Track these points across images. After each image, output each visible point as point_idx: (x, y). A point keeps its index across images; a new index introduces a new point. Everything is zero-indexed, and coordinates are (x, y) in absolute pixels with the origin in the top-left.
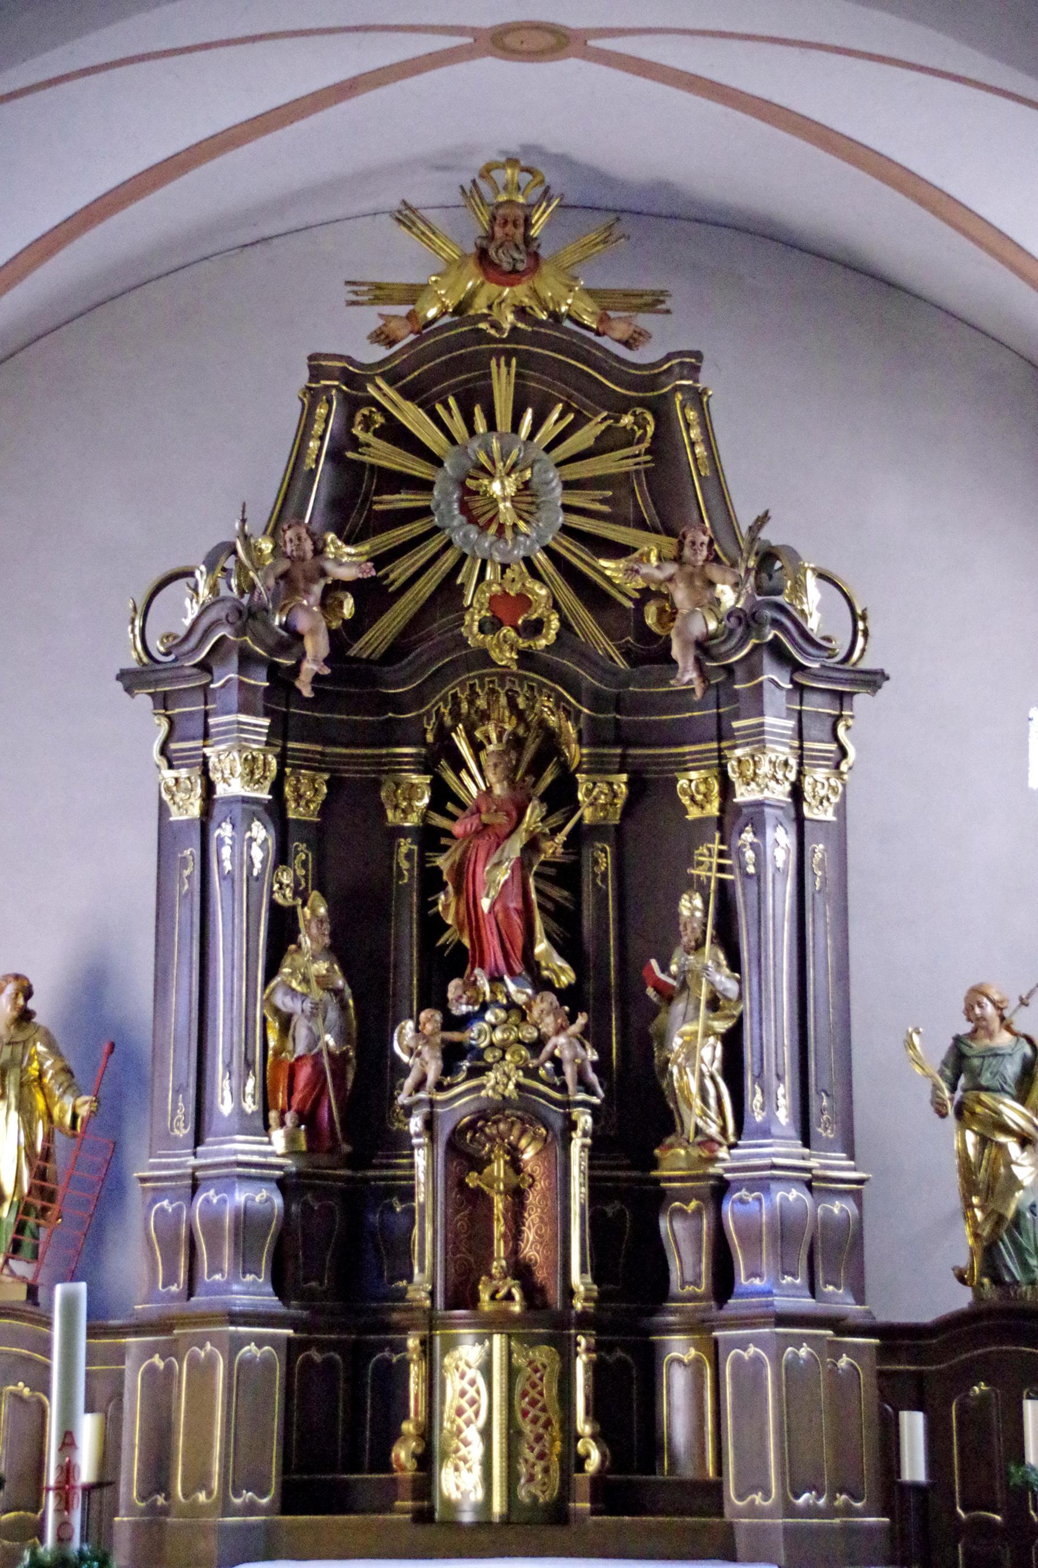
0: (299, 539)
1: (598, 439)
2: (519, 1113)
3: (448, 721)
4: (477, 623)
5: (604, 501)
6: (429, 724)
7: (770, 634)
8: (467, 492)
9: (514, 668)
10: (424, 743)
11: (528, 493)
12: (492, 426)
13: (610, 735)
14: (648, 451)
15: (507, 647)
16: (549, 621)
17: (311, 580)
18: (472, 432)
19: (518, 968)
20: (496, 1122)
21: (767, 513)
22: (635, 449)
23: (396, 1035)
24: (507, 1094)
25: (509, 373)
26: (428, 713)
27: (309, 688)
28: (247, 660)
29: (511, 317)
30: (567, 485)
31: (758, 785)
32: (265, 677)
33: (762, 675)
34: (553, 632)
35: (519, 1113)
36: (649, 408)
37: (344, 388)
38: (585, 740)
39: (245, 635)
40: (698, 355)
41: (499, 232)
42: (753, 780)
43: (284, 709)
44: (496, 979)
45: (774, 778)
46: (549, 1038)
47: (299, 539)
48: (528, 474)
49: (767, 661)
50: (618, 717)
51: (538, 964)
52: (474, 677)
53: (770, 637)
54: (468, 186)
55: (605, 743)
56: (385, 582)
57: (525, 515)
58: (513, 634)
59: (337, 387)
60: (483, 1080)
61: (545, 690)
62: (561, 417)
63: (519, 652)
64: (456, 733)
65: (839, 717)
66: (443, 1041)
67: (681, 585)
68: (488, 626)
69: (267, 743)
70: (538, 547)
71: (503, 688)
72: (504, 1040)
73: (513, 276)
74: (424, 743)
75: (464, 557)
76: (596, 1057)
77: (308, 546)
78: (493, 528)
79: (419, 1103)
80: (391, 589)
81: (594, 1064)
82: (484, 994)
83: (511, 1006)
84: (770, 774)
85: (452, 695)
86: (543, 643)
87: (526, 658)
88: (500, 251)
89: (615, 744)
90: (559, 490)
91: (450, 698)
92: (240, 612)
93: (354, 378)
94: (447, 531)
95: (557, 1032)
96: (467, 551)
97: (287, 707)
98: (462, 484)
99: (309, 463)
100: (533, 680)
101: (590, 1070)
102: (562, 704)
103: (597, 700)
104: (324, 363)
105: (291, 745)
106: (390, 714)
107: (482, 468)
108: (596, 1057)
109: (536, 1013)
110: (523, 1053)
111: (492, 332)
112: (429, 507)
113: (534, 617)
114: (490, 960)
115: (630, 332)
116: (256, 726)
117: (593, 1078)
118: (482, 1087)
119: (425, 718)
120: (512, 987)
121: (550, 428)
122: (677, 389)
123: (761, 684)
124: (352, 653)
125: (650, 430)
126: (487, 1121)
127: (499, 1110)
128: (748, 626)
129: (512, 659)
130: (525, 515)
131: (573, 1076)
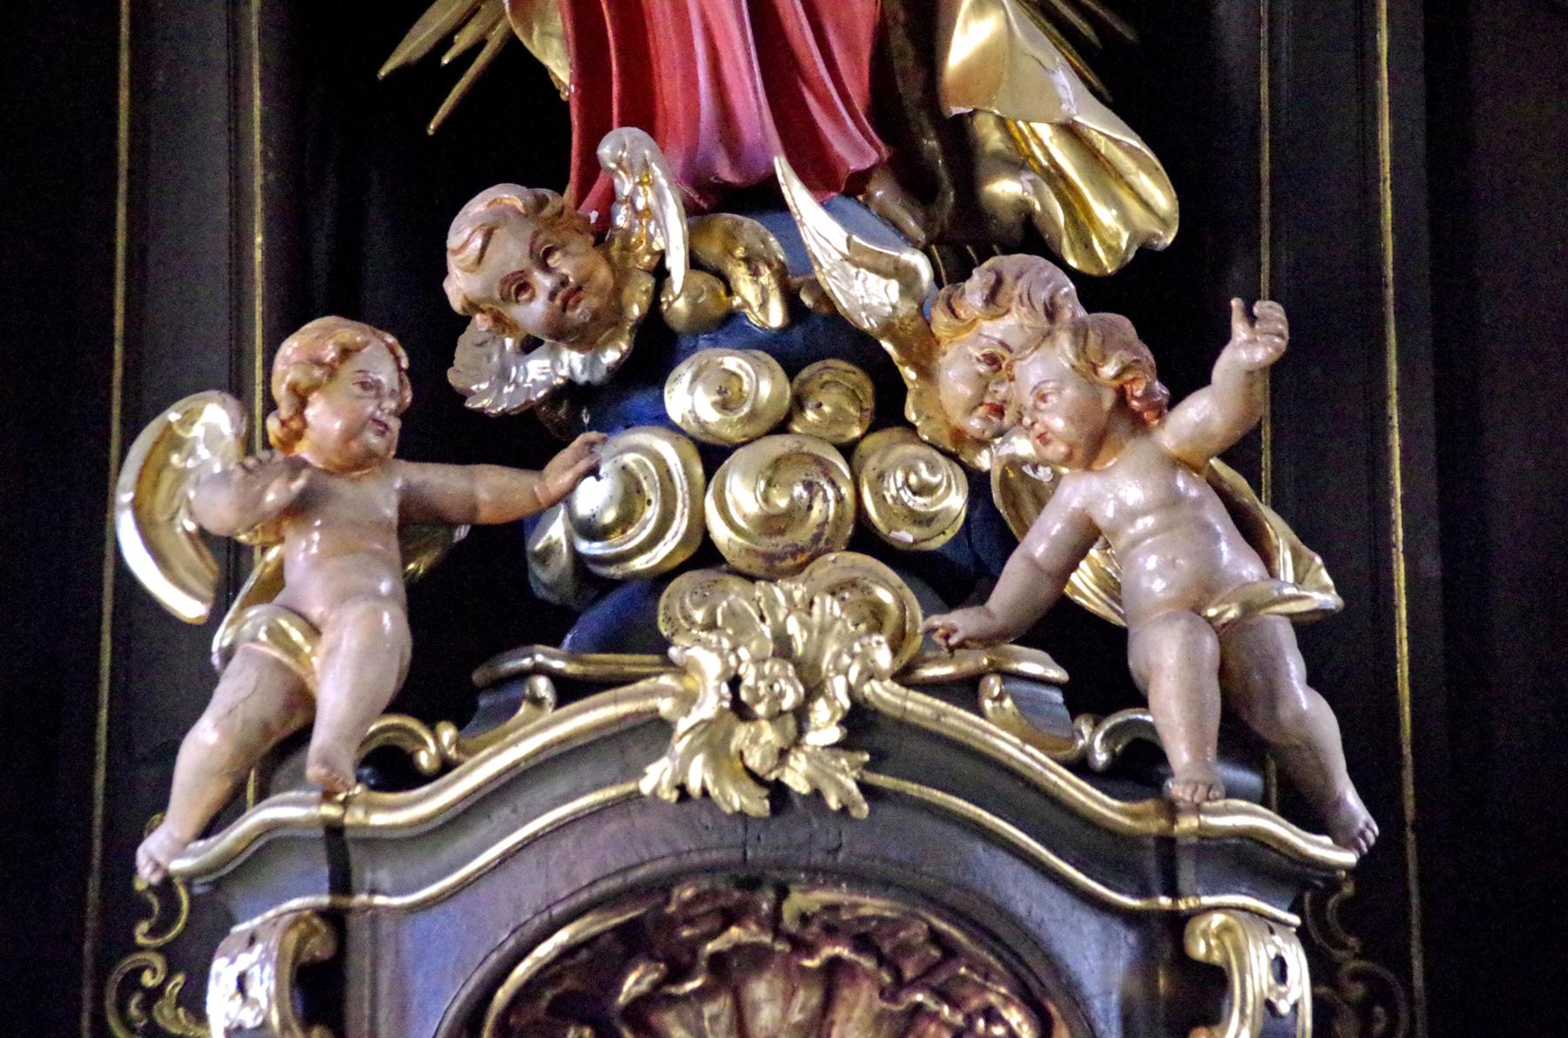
2: (873, 905)
19: (854, 148)
20: (727, 973)
23: (125, 497)
24: (796, 777)
35: (873, 905)
44: (729, 197)
46: (1040, 496)
51: (958, 134)
60: (656, 695)
66: (416, 521)
72: (772, 523)
76: (1323, 596)
79: (273, 842)
81: (1310, 630)
82: (660, 273)
83: (815, 334)
95: (1093, 448)
101: (1295, 667)
108: (1323, 596)
109: (956, 375)
110: (885, 596)
114: (681, 85)
117: (1311, 713)
118: (652, 732)
120: (818, 225)
126: (678, 973)
127: (745, 884)
131: (1193, 696)
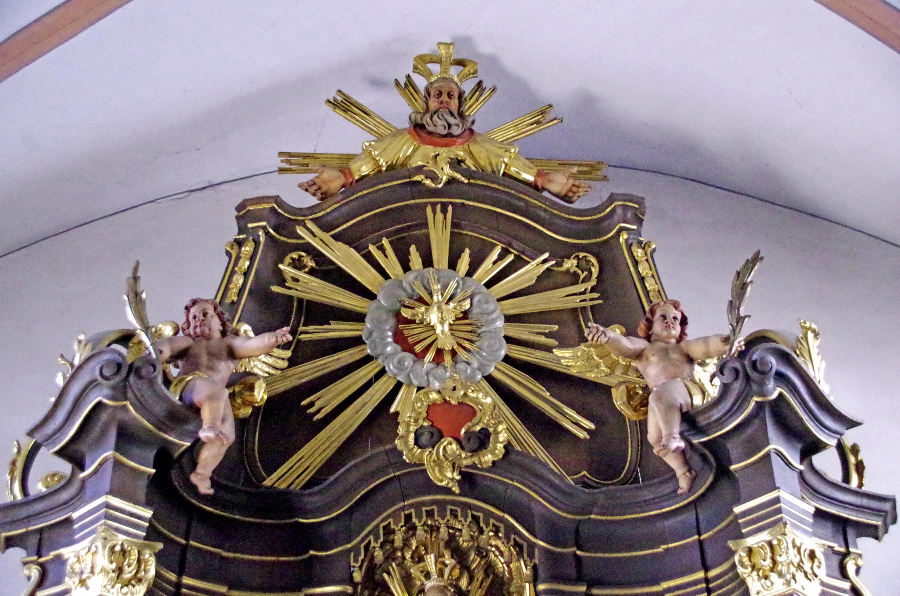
0: (205, 315)
1: (540, 278)
3: (379, 555)
4: (413, 435)
5: (547, 336)
6: (356, 561)
7: (775, 391)
8: (400, 319)
9: (456, 490)
10: (351, 581)
11: (467, 322)
12: (428, 262)
13: (572, 572)
14: (593, 290)
15: (447, 465)
16: (497, 433)
17: (214, 356)
18: (406, 268)
21: (759, 253)
22: (581, 288)
25: (445, 218)
26: (356, 549)
27: (208, 484)
28: (127, 438)
29: (447, 170)
30: (509, 319)
31: (781, 575)
32: (152, 462)
33: (768, 444)
34: (500, 446)
36: (594, 255)
37: (271, 231)
38: (541, 574)
39: (126, 399)
40: (640, 201)
41: (434, 104)
42: (772, 570)
43: (184, 542)
45: (800, 567)
47: (205, 315)
48: (467, 305)
49: (772, 432)
50: (579, 553)
52: (411, 506)
53: (774, 396)
54: (403, 81)
55: (567, 581)
56: (312, 410)
57: (467, 345)
58: (455, 446)
59: (264, 228)
61: (492, 521)
62: (501, 257)
63: (461, 473)
64: (389, 574)
65: (848, 554)
67: (654, 359)
68: (425, 439)
69: (146, 539)
70: (480, 377)
71: (443, 519)
73: (449, 139)
74: (351, 581)
75: (399, 386)
77: (216, 325)
78: (430, 356)
80: (316, 418)
84: (796, 561)
85: (384, 528)
86: (488, 458)
87: (469, 480)
88: (435, 117)
89: (579, 580)
90: (500, 323)
91: (382, 532)
92: (119, 367)
93: (284, 221)
94: (380, 361)
96: (400, 379)
97: (187, 539)
98: (398, 315)
99: (233, 296)
100: (480, 509)
102: (513, 537)
103: (554, 532)
104: (252, 208)
105: (187, 581)
106: (312, 552)
107: (421, 300)
111: (428, 182)
112: (361, 337)
113: (478, 428)
115: (570, 185)
116: (132, 515)
119: (353, 554)
121: (488, 269)
122: (622, 230)
123: (768, 456)
124: (268, 483)
125: (595, 271)
128: (748, 378)
129: (453, 479)
130: (467, 345)
